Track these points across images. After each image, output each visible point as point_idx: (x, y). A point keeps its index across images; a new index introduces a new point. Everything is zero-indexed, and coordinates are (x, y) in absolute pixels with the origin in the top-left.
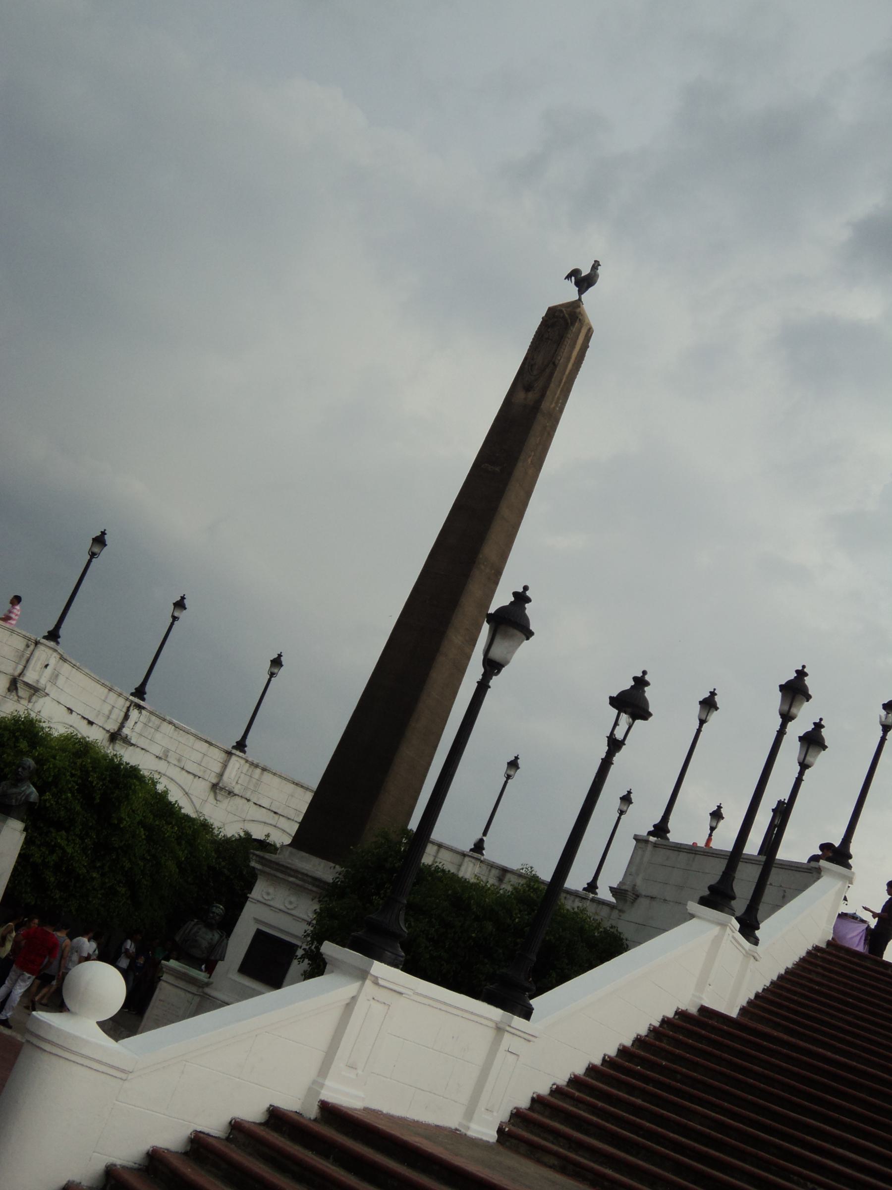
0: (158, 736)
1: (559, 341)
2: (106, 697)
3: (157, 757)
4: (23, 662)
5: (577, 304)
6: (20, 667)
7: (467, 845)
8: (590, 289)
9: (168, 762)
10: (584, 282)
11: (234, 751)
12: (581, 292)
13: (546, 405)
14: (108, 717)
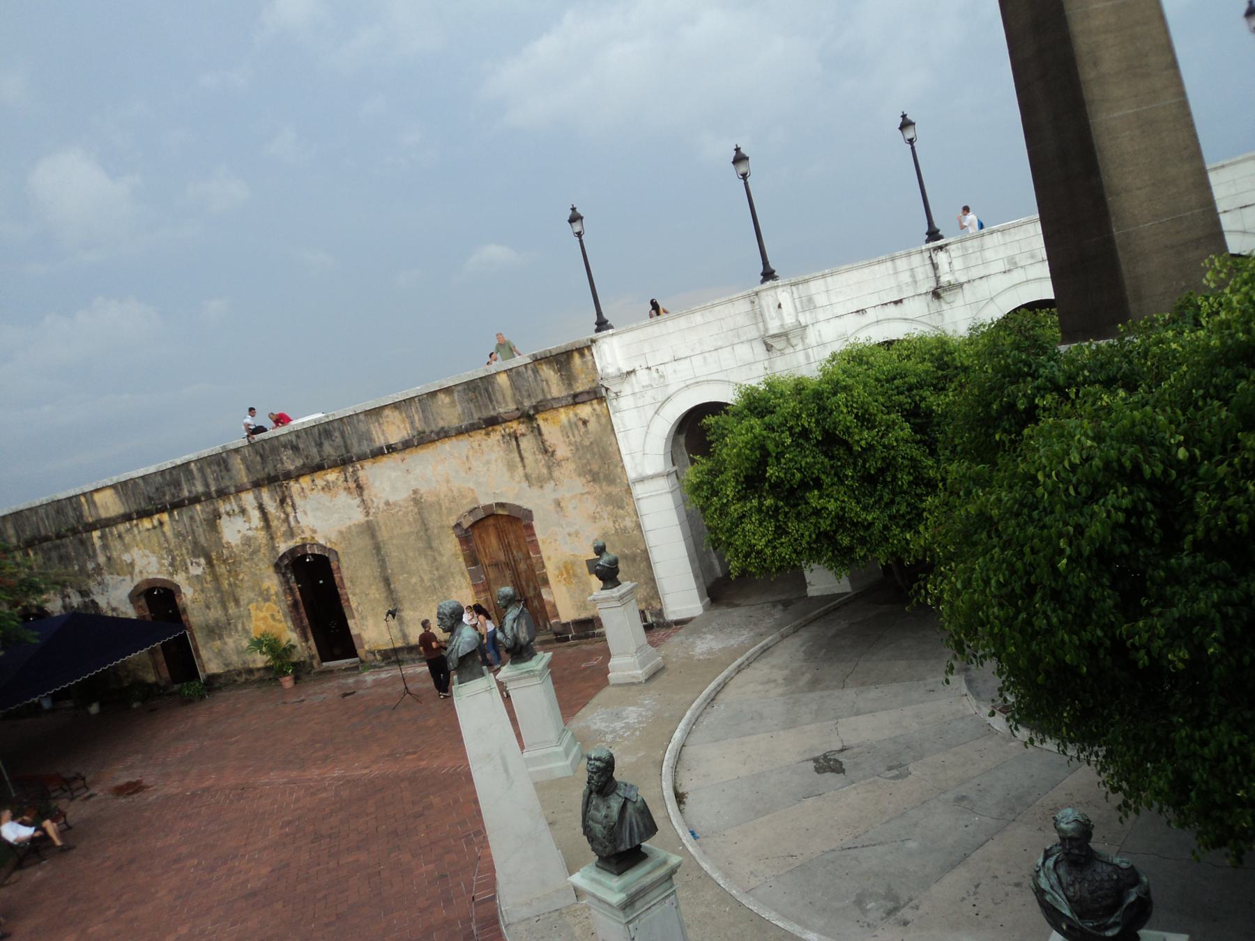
0: (989, 255)
2: (895, 268)
3: (1005, 272)
4: (760, 319)
6: (761, 325)
9: (1022, 267)
14: (915, 282)
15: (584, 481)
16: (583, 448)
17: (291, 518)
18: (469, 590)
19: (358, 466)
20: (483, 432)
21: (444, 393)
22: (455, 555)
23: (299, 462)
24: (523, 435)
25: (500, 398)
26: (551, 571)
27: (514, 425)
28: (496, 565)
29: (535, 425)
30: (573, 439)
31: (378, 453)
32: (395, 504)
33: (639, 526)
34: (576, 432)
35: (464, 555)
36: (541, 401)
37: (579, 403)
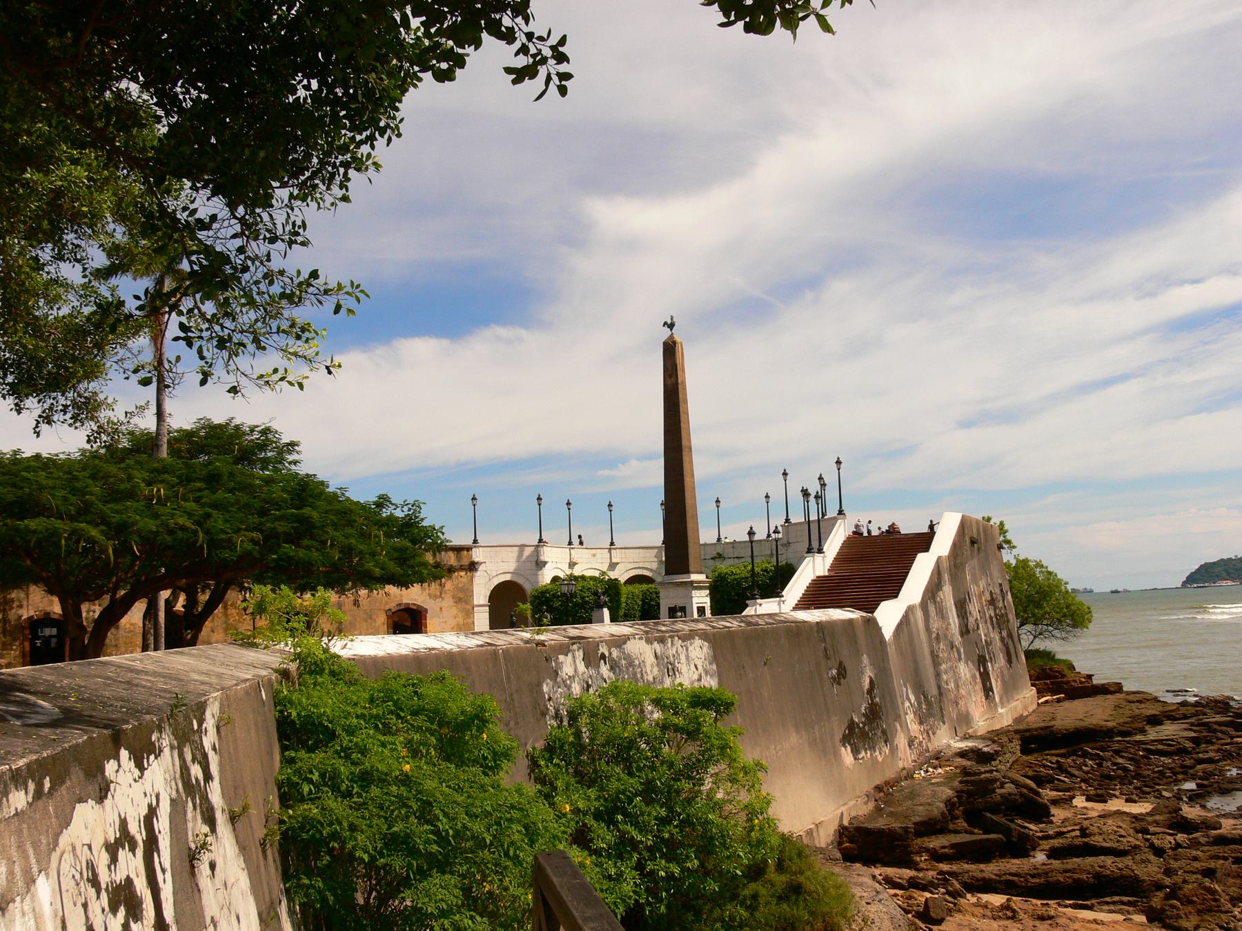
5: (672, 336)
7: (715, 541)
12: (671, 330)
13: (679, 381)
33: (474, 622)
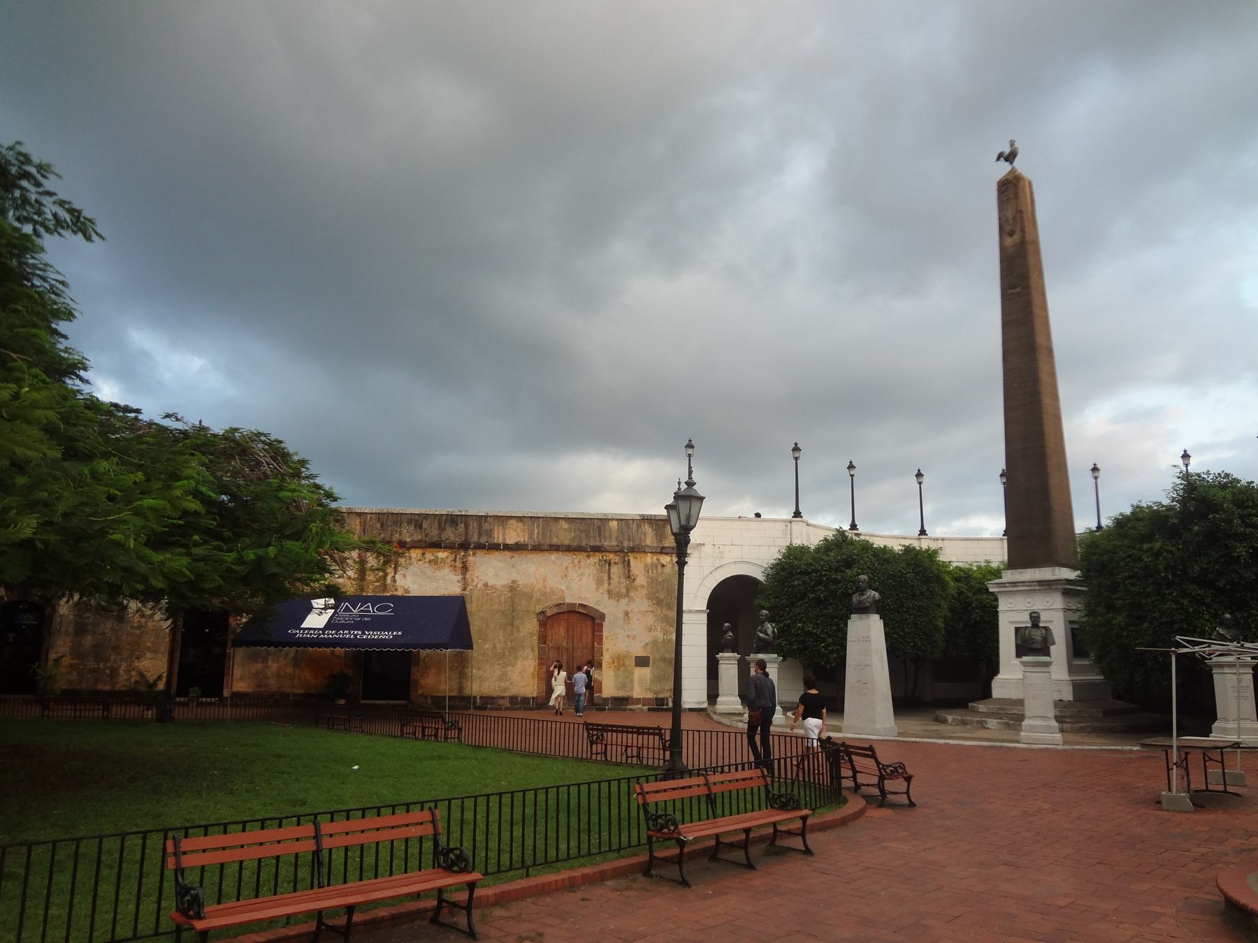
1: (1016, 196)
5: (1013, 171)
8: (1016, 158)
10: (1010, 157)
11: (921, 537)
12: (1011, 163)
13: (1029, 238)
15: (651, 603)
16: (656, 582)
17: (389, 578)
18: (533, 661)
19: (471, 553)
20: (586, 554)
21: (565, 521)
22: (532, 634)
23: (417, 537)
24: (616, 563)
25: (607, 534)
26: (606, 658)
27: (611, 556)
28: (558, 648)
29: (627, 560)
30: (651, 575)
31: (495, 547)
32: (493, 587)
34: (655, 571)
35: (539, 636)
36: (637, 545)
37: (663, 553)
